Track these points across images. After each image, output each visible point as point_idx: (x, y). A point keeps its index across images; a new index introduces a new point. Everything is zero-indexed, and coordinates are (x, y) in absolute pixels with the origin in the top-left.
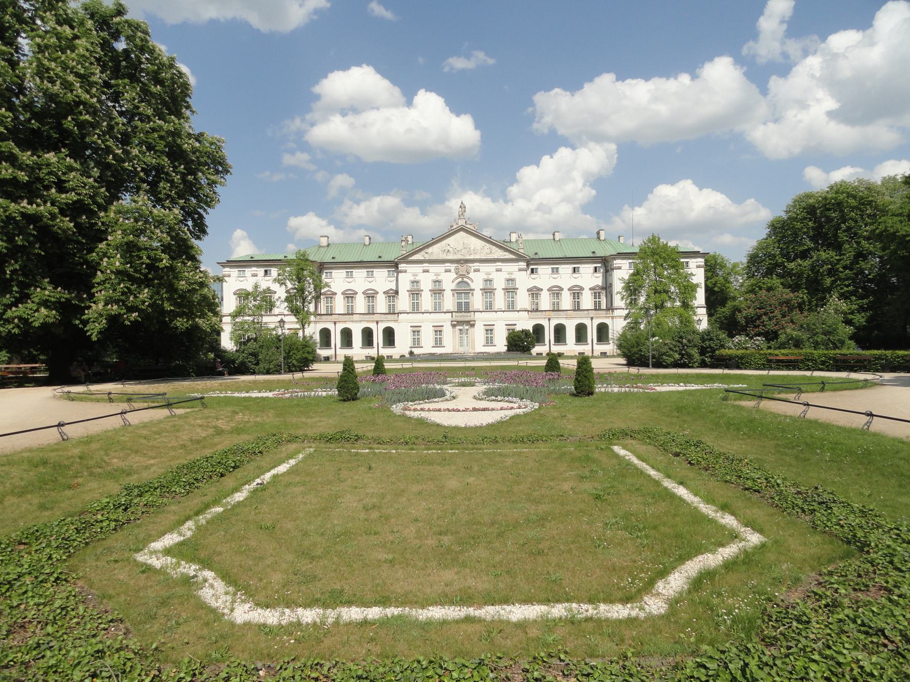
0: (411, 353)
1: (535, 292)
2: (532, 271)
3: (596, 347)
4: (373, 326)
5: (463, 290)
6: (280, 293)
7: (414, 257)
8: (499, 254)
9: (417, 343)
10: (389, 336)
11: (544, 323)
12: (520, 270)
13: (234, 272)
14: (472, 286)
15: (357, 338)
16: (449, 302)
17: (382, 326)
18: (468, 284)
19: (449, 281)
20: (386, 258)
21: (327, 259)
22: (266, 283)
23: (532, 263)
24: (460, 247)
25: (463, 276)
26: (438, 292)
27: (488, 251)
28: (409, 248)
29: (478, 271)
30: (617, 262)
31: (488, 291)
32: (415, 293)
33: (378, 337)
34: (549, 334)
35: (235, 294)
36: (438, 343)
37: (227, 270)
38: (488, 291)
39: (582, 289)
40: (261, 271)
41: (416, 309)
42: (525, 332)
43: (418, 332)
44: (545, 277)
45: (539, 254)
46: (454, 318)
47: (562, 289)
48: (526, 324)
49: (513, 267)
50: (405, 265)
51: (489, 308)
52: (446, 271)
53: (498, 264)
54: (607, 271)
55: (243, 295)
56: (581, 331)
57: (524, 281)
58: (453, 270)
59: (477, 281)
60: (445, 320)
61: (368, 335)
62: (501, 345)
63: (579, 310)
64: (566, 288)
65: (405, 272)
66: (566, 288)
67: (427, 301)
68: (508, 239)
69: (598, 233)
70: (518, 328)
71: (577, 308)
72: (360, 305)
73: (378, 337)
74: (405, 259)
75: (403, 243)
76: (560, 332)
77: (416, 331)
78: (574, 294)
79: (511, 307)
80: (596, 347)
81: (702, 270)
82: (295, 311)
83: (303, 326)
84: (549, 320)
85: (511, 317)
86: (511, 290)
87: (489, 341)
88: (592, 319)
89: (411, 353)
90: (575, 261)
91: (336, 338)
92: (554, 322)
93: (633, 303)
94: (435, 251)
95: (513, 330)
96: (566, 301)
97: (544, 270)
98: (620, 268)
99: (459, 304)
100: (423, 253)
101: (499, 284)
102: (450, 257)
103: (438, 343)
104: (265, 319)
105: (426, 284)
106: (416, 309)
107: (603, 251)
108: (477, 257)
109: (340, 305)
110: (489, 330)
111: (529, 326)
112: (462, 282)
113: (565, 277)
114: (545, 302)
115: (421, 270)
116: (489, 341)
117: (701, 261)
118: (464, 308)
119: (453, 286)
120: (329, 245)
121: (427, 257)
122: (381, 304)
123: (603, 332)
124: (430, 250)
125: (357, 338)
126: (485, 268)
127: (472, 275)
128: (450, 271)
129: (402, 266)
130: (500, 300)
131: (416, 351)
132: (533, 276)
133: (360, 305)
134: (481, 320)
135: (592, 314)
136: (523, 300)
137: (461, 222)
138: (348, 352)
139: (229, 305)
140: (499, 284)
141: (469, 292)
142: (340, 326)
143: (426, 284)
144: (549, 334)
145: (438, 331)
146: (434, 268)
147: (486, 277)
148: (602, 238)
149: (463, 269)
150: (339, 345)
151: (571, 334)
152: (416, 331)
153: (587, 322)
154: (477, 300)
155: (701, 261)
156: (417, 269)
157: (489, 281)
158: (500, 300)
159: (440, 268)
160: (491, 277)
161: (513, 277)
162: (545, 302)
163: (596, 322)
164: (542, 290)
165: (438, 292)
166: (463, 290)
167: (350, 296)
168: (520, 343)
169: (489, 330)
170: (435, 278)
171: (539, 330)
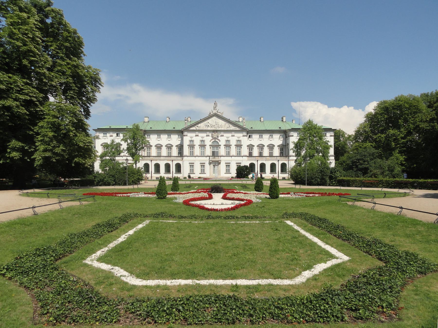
0: (189, 177)
1: (251, 147)
2: (250, 137)
3: (280, 175)
4: (170, 162)
5: (215, 145)
6: (124, 146)
7: (191, 129)
8: (232, 128)
9: (192, 171)
10: (178, 168)
11: (255, 162)
12: (243, 136)
13: (101, 135)
14: (220, 144)
15: (162, 169)
16: (208, 151)
17: (175, 162)
19: (208, 141)
20: (177, 128)
21: (148, 128)
22: (118, 140)
23: (250, 133)
24: (214, 124)
25: (215, 138)
26: (203, 146)
27: (228, 126)
28: (189, 124)
29: (223, 136)
30: (292, 133)
31: (228, 146)
32: (192, 146)
33: (173, 168)
34: (257, 169)
35: (101, 145)
36: (203, 172)
37: (98, 134)
38: (228, 146)
39: (274, 146)
40: (115, 135)
41: (192, 155)
42: (246, 167)
43: (193, 166)
44: (256, 140)
45: (253, 128)
46: (210, 159)
47: (264, 146)
48: (246, 162)
49: (240, 135)
51: (228, 155)
52: (207, 136)
54: (286, 137)
55: (105, 146)
56: (273, 167)
57: (245, 141)
58: (210, 135)
59: (222, 141)
60: (206, 160)
61: (168, 167)
62: (234, 173)
63: (272, 156)
64: (266, 145)
66: (266, 145)
67: (197, 150)
68: (237, 120)
69: (282, 118)
70: (242, 165)
71: (271, 155)
72: (164, 152)
73: (173, 168)
74: (187, 129)
75: (186, 121)
76: (263, 167)
77: (192, 165)
78: (270, 148)
79: (239, 155)
80: (280, 175)
81: (333, 137)
82: (133, 155)
83: (136, 162)
84: (257, 161)
85: (239, 159)
86: (239, 146)
87: (228, 171)
88: (278, 161)
89: (189, 177)
90: (271, 132)
91: (152, 168)
92: (260, 162)
93: (298, 154)
94: (202, 126)
95: (240, 166)
96: (266, 152)
97: (255, 137)
98: (292, 136)
99: (213, 152)
100: (196, 127)
101: (233, 142)
102: (209, 129)
103: (203, 172)
104: (117, 158)
105: (197, 142)
106: (192, 155)
107: (285, 127)
108: (223, 129)
109: (154, 152)
110: (228, 165)
111: (248, 164)
112: (215, 141)
113: (266, 140)
114: (256, 152)
116: (228, 171)
117: (332, 134)
118: (214, 154)
119: (210, 143)
120: (148, 122)
121: (198, 128)
122: (175, 152)
123: (283, 166)
124: (199, 125)
125: (162, 169)
126: (226, 135)
128: (209, 136)
129: (185, 133)
130: (233, 151)
131: (192, 176)
132: (250, 139)
133: (164, 152)
134: (224, 160)
135: (279, 158)
136: (245, 151)
137: (215, 112)
138: (158, 175)
139: (99, 150)
140: (233, 142)
141: (218, 146)
142: (154, 162)
143: (197, 142)
144: (257, 169)
145: (203, 165)
146: (201, 135)
147: (226, 139)
148: (284, 120)
149: (215, 135)
150: (153, 172)
151: (268, 168)
152: (192, 165)
153: (276, 162)
154: (222, 151)
155: (332, 134)
156: (193, 135)
157: (228, 141)
158: (233, 151)
160: (229, 139)
161: (240, 139)
162: (256, 152)
163: (281, 162)
164: (254, 146)
165: (203, 146)
166: (215, 145)
167: (159, 147)
168: (242, 172)
169: (228, 165)
170: (201, 139)
171: (252, 166)
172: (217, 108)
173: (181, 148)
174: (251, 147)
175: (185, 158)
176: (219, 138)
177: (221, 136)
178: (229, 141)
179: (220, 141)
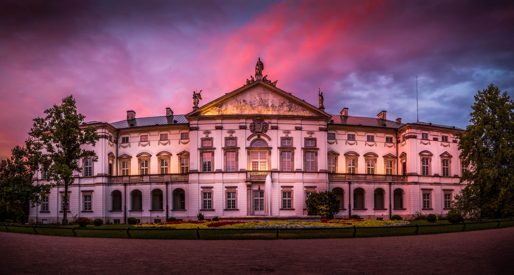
14: (270, 144)
18: (267, 144)
29: (276, 128)
50: (196, 122)
52: (241, 128)
53: (299, 122)
58: (248, 128)
65: (197, 129)
101: (298, 143)
112: (259, 139)
115: (213, 127)
126: (284, 126)
127: (267, 134)
140: (298, 143)
156: (211, 127)
159: (234, 125)
172: (264, 73)
173: (184, 156)
174: (333, 155)
175: (193, 177)
176: (267, 134)
177: (273, 128)
178: (290, 139)
179: (270, 139)
